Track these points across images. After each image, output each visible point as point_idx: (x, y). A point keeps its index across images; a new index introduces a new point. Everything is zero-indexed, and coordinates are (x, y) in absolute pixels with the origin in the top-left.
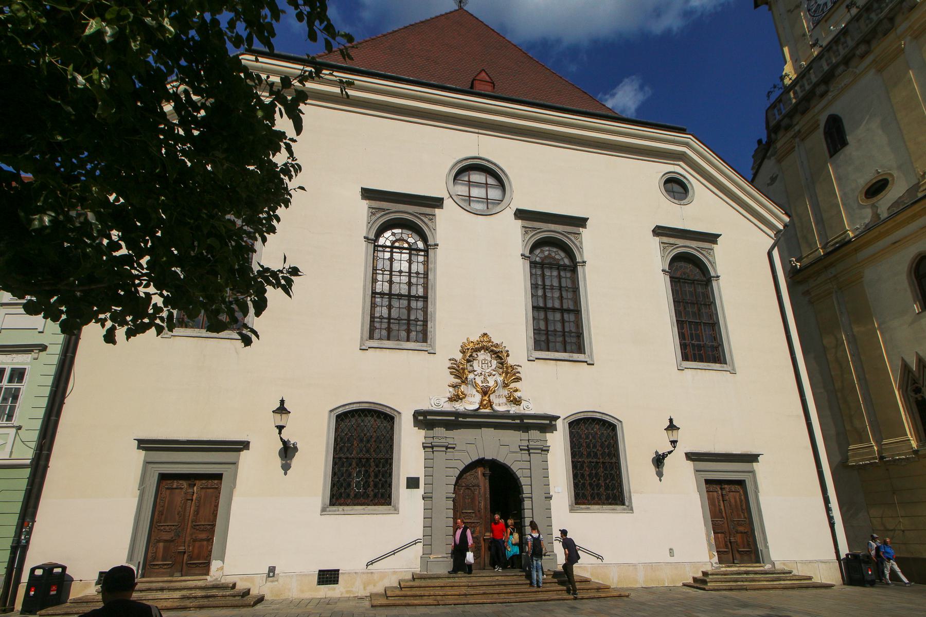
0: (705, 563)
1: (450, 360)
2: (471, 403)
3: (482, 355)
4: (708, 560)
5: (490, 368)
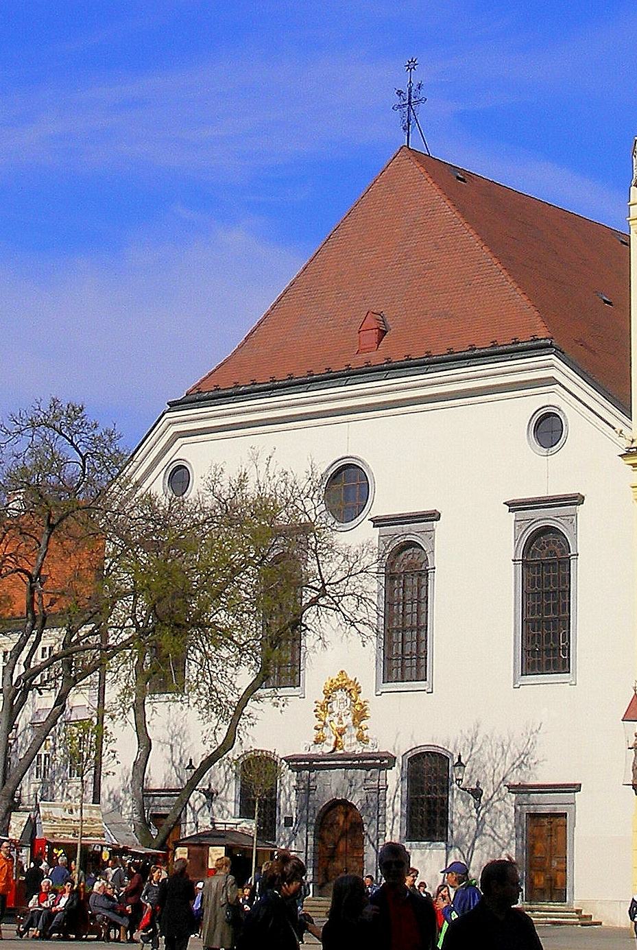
1: (316, 702)
3: (340, 695)
5: (346, 708)
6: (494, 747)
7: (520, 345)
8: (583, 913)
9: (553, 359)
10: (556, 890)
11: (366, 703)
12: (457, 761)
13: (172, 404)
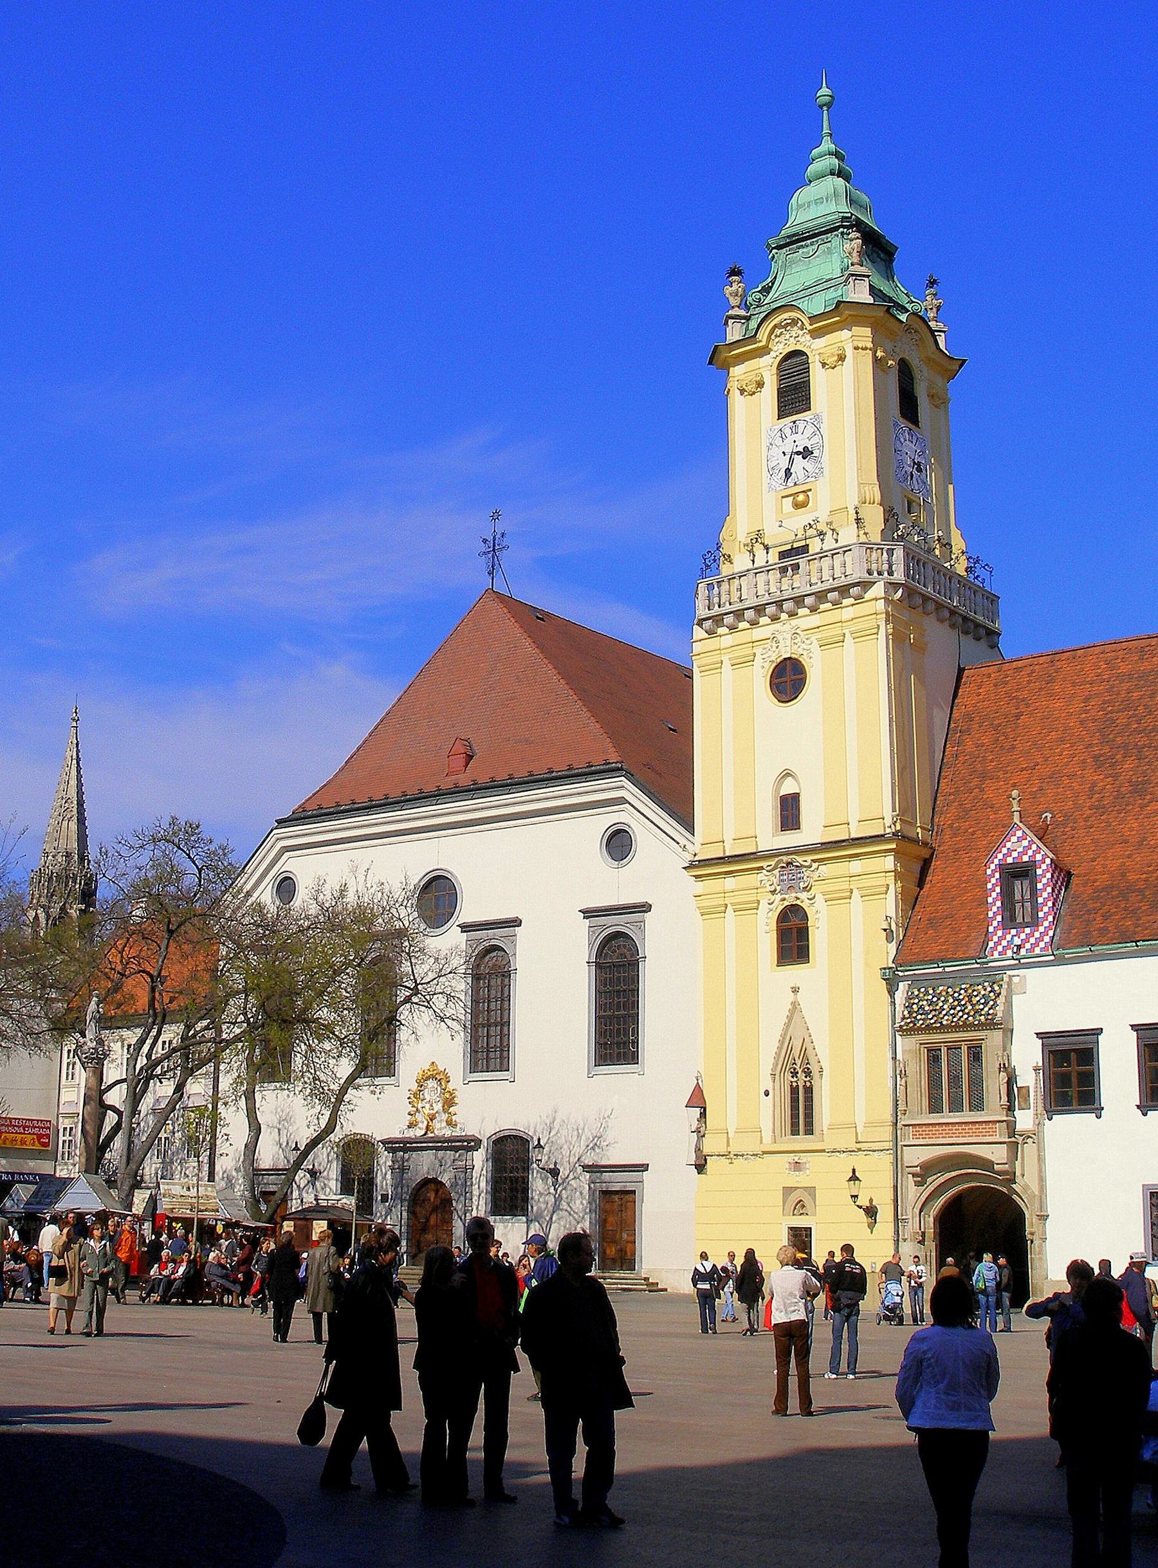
3: (431, 1084)
6: (570, 1131)
7: (593, 768)
8: (651, 1281)
9: (624, 781)
10: (626, 1259)
12: (536, 1143)
13: (278, 821)
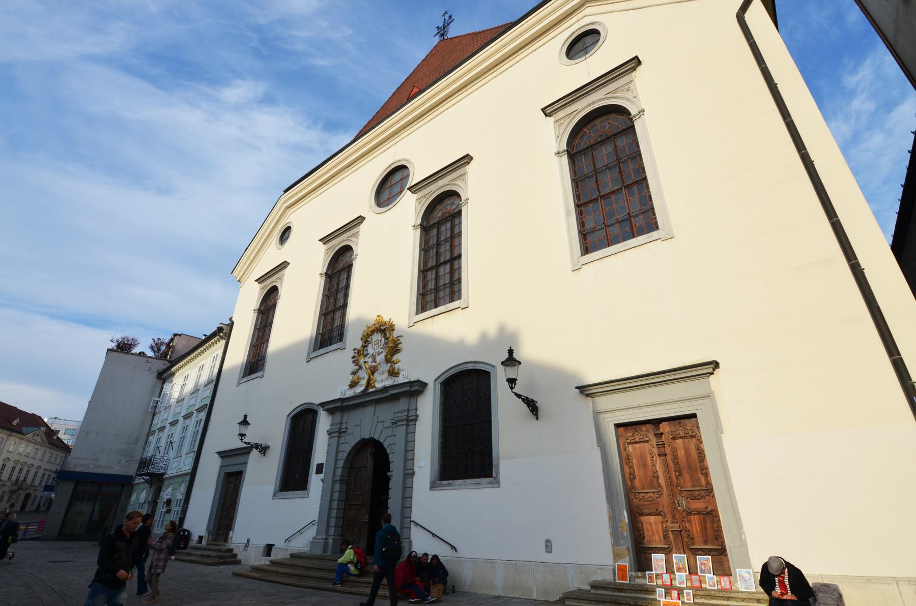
0: (602, 568)
1: (354, 350)
2: (361, 386)
4: (612, 563)
11: (398, 338)
